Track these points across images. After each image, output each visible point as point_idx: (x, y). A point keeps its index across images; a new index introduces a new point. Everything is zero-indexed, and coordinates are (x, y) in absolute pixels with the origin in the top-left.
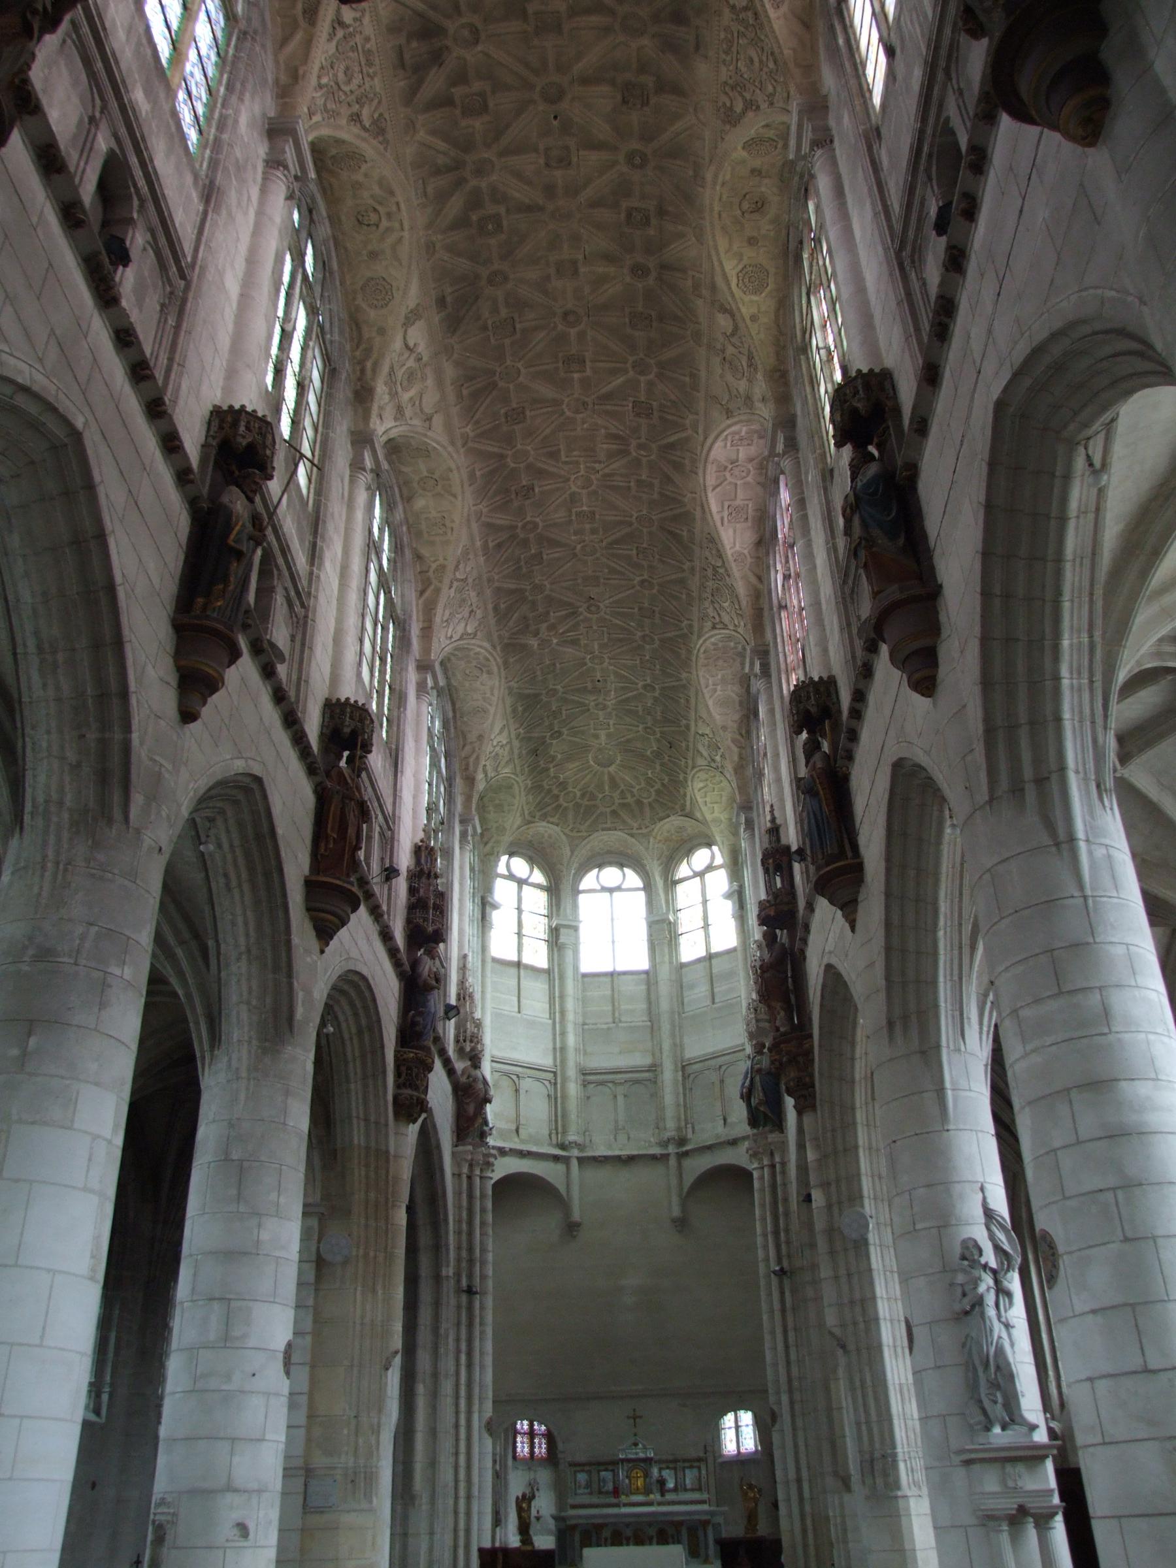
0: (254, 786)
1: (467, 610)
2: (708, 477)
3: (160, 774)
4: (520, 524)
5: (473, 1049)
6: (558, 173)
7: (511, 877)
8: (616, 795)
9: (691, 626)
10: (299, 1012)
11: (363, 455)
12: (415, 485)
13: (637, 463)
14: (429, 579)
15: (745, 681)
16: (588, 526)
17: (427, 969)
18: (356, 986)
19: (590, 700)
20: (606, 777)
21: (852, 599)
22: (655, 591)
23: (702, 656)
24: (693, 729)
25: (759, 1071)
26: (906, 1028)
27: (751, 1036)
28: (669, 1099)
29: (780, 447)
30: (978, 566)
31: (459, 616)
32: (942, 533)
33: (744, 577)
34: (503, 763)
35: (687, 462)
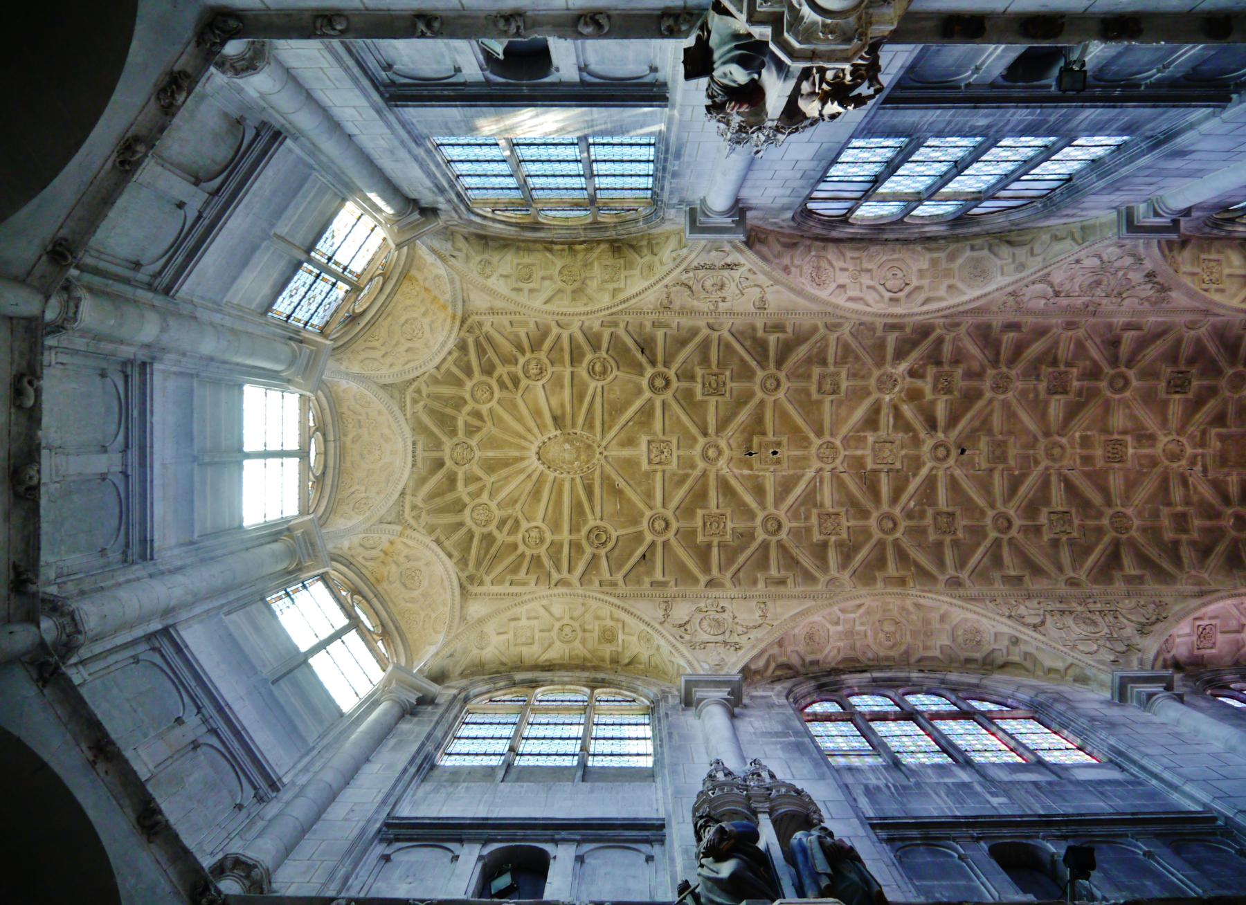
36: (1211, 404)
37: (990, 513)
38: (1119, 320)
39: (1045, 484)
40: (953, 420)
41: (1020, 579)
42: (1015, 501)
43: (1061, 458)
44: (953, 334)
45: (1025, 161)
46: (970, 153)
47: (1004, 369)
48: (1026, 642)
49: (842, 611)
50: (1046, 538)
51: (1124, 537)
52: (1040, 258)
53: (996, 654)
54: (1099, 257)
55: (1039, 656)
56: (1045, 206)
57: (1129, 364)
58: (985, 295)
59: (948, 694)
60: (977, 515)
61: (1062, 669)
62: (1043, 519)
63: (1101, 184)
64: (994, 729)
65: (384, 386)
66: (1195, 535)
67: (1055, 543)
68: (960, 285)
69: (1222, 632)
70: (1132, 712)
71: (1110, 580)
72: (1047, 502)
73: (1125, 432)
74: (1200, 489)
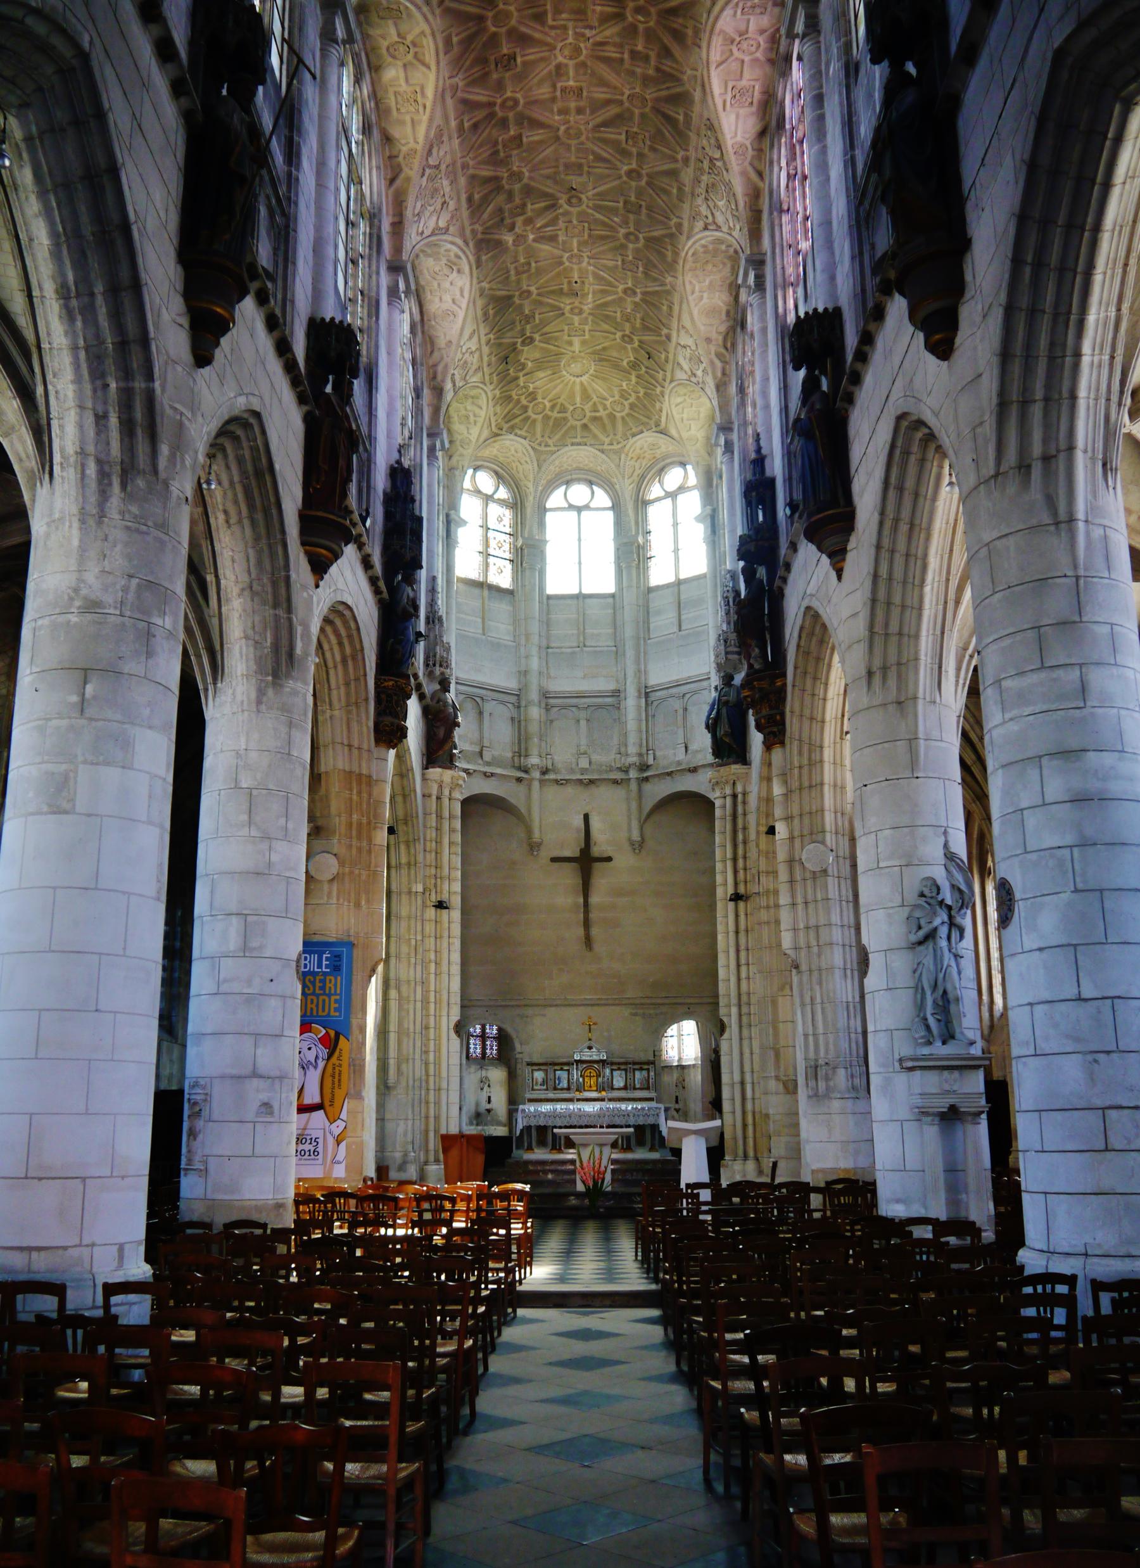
0: (252, 420)
1: (440, 201)
2: (712, 54)
3: (181, 425)
4: (499, 101)
5: (442, 674)
7: (478, 492)
8: (588, 407)
9: (679, 226)
10: (298, 650)
11: (334, 23)
12: (384, 52)
13: (632, 30)
14: (399, 165)
15: (734, 290)
16: (573, 105)
17: (405, 597)
18: (341, 615)
19: (566, 304)
20: (578, 388)
21: (867, 223)
22: (643, 183)
23: (690, 258)
24: (674, 339)
25: (727, 702)
26: (884, 678)
27: (719, 667)
28: (631, 725)
29: (800, 27)
30: (1012, 231)
31: (432, 209)
32: (977, 182)
33: (744, 173)
34: (471, 373)
35: (690, 32)
36: (524, 29)
40: (546, 195)
49: (693, 293)
65: (539, 466)
73: (554, 86)
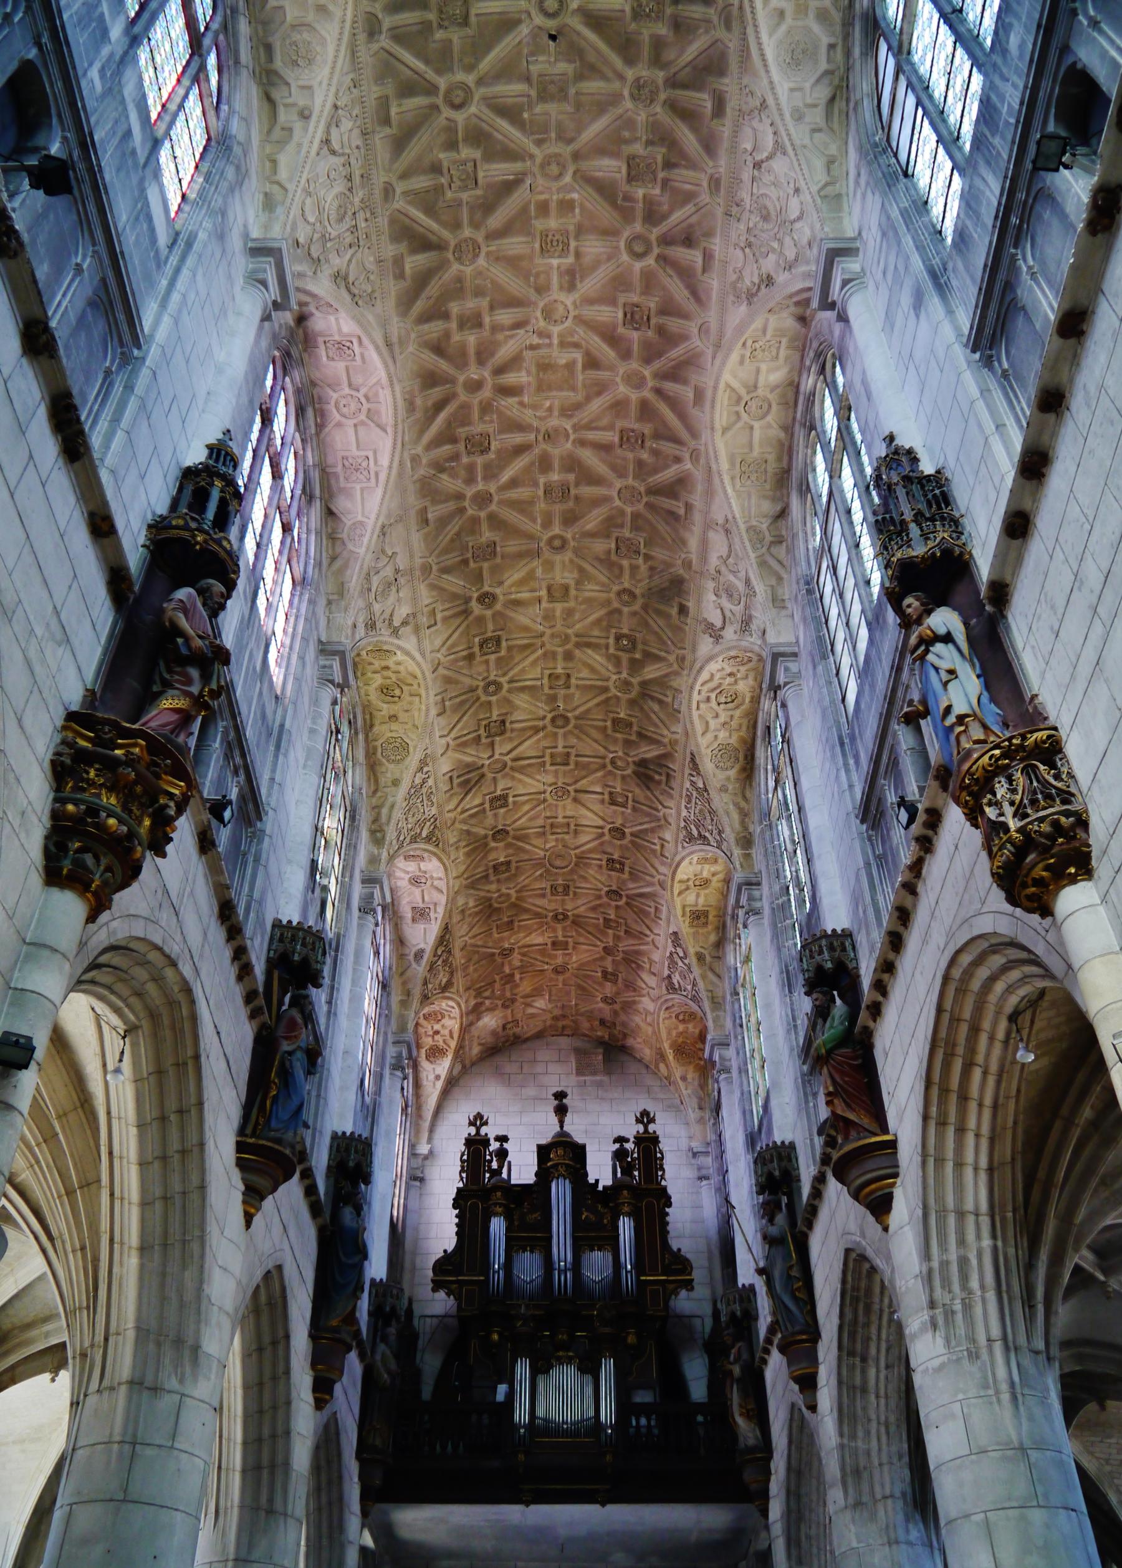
2: (390, 400)
6: (559, 671)
13: (482, 357)
37: (470, 79)
38: (717, 245)
39: (509, 154)
41: (386, 121)
42: (488, 114)
43: (546, 176)
44: (715, 19)
45: (942, 112)
46: (970, 31)
47: (663, 96)
48: (306, 130)
50: (442, 156)
51: (450, 256)
52: (807, 141)
53: (284, 88)
54: (799, 218)
55: (291, 148)
56: (876, 145)
57: (662, 259)
58: (766, 66)
59: (219, 18)
60: (467, 60)
61: (277, 178)
62: (467, 152)
63: (895, 213)
64: (186, 82)
66: (456, 337)
67: (436, 169)
68: (783, 28)
69: (347, 368)
70: (241, 264)
71: (395, 238)
72: (489, 157)
73: (578, 255)
74: (511, 342)
